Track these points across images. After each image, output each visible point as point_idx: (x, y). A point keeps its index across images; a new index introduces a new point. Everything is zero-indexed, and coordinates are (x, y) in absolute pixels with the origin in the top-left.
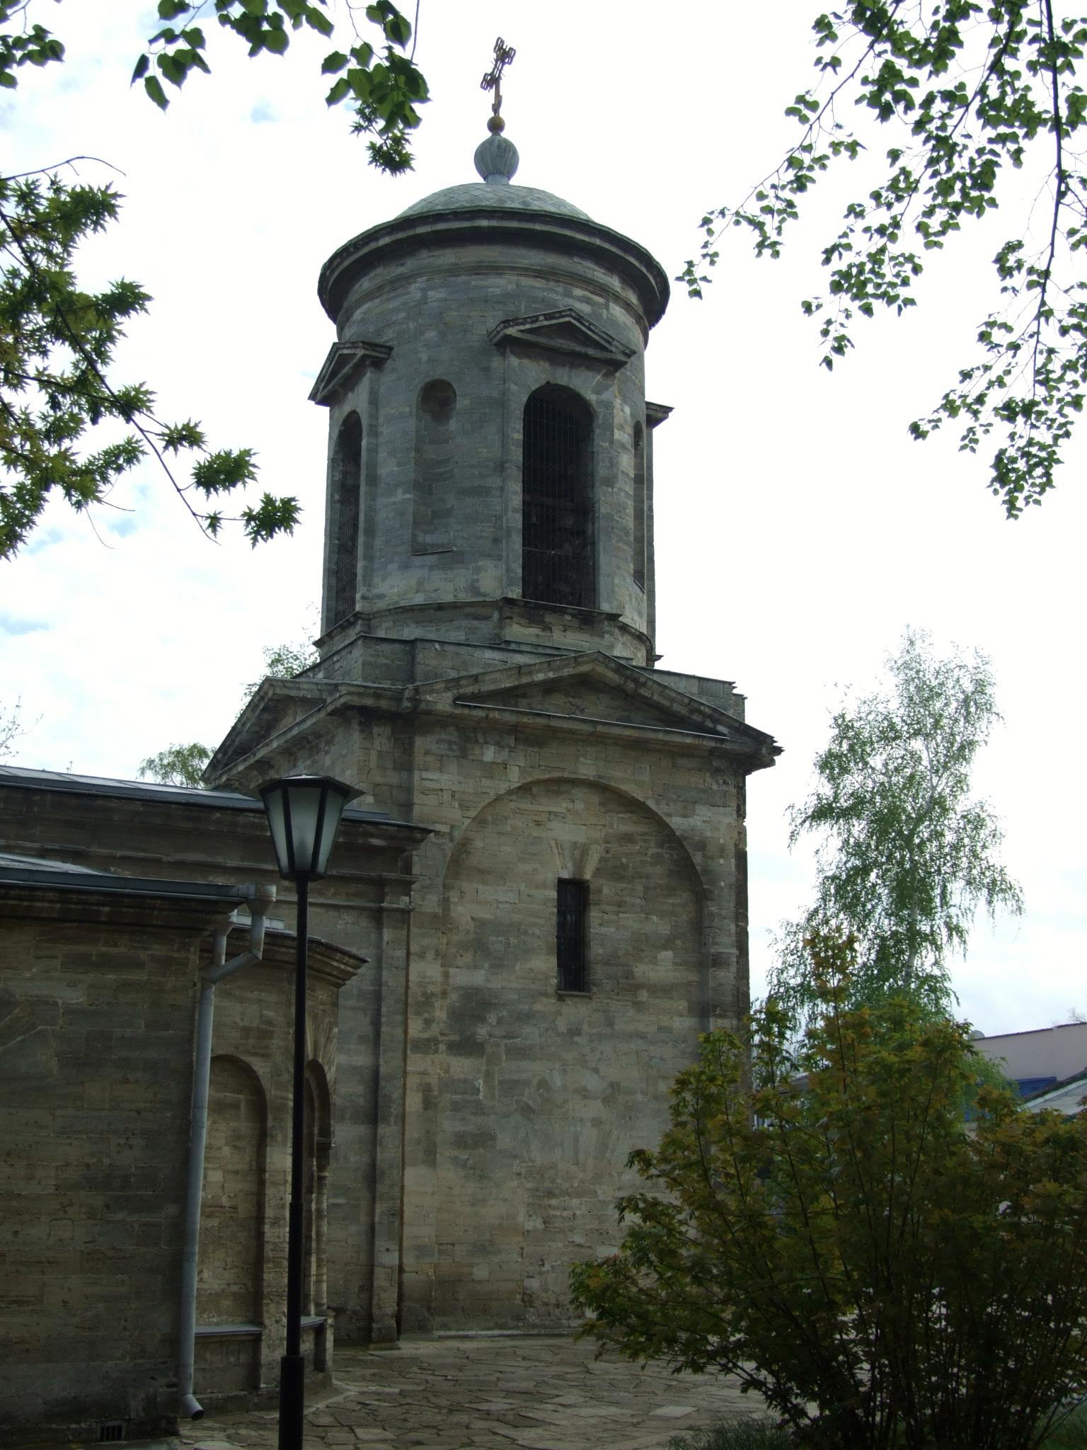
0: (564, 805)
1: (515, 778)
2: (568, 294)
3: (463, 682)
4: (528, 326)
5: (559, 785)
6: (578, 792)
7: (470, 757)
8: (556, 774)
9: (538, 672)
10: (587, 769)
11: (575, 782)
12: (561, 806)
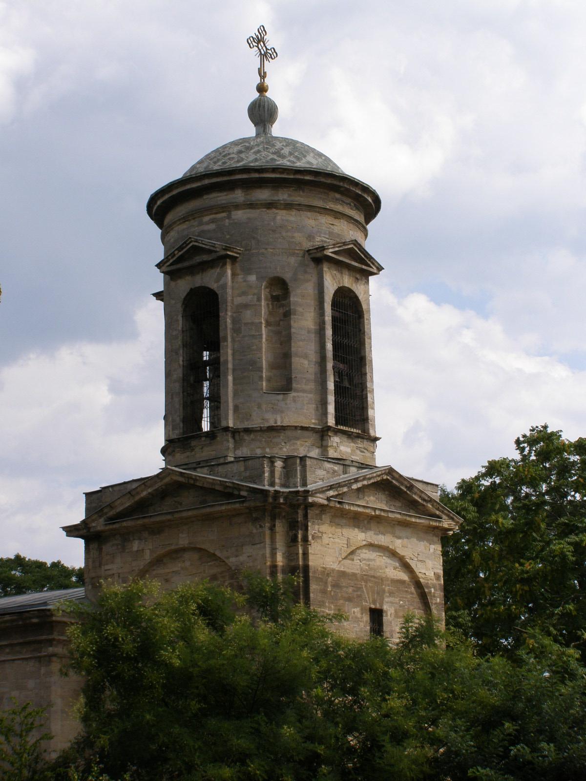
0: (180, 565)
1: (148, 557)
2: (201, 224)
3: (105, 510)
4: (171, 261)
5: (176, 554)
6: (187, 555)
7: (127, 551)
8: (168, 548)
9: (142, 491)
10: (183, 540)
11: (184, 550)
12: (177, 566)
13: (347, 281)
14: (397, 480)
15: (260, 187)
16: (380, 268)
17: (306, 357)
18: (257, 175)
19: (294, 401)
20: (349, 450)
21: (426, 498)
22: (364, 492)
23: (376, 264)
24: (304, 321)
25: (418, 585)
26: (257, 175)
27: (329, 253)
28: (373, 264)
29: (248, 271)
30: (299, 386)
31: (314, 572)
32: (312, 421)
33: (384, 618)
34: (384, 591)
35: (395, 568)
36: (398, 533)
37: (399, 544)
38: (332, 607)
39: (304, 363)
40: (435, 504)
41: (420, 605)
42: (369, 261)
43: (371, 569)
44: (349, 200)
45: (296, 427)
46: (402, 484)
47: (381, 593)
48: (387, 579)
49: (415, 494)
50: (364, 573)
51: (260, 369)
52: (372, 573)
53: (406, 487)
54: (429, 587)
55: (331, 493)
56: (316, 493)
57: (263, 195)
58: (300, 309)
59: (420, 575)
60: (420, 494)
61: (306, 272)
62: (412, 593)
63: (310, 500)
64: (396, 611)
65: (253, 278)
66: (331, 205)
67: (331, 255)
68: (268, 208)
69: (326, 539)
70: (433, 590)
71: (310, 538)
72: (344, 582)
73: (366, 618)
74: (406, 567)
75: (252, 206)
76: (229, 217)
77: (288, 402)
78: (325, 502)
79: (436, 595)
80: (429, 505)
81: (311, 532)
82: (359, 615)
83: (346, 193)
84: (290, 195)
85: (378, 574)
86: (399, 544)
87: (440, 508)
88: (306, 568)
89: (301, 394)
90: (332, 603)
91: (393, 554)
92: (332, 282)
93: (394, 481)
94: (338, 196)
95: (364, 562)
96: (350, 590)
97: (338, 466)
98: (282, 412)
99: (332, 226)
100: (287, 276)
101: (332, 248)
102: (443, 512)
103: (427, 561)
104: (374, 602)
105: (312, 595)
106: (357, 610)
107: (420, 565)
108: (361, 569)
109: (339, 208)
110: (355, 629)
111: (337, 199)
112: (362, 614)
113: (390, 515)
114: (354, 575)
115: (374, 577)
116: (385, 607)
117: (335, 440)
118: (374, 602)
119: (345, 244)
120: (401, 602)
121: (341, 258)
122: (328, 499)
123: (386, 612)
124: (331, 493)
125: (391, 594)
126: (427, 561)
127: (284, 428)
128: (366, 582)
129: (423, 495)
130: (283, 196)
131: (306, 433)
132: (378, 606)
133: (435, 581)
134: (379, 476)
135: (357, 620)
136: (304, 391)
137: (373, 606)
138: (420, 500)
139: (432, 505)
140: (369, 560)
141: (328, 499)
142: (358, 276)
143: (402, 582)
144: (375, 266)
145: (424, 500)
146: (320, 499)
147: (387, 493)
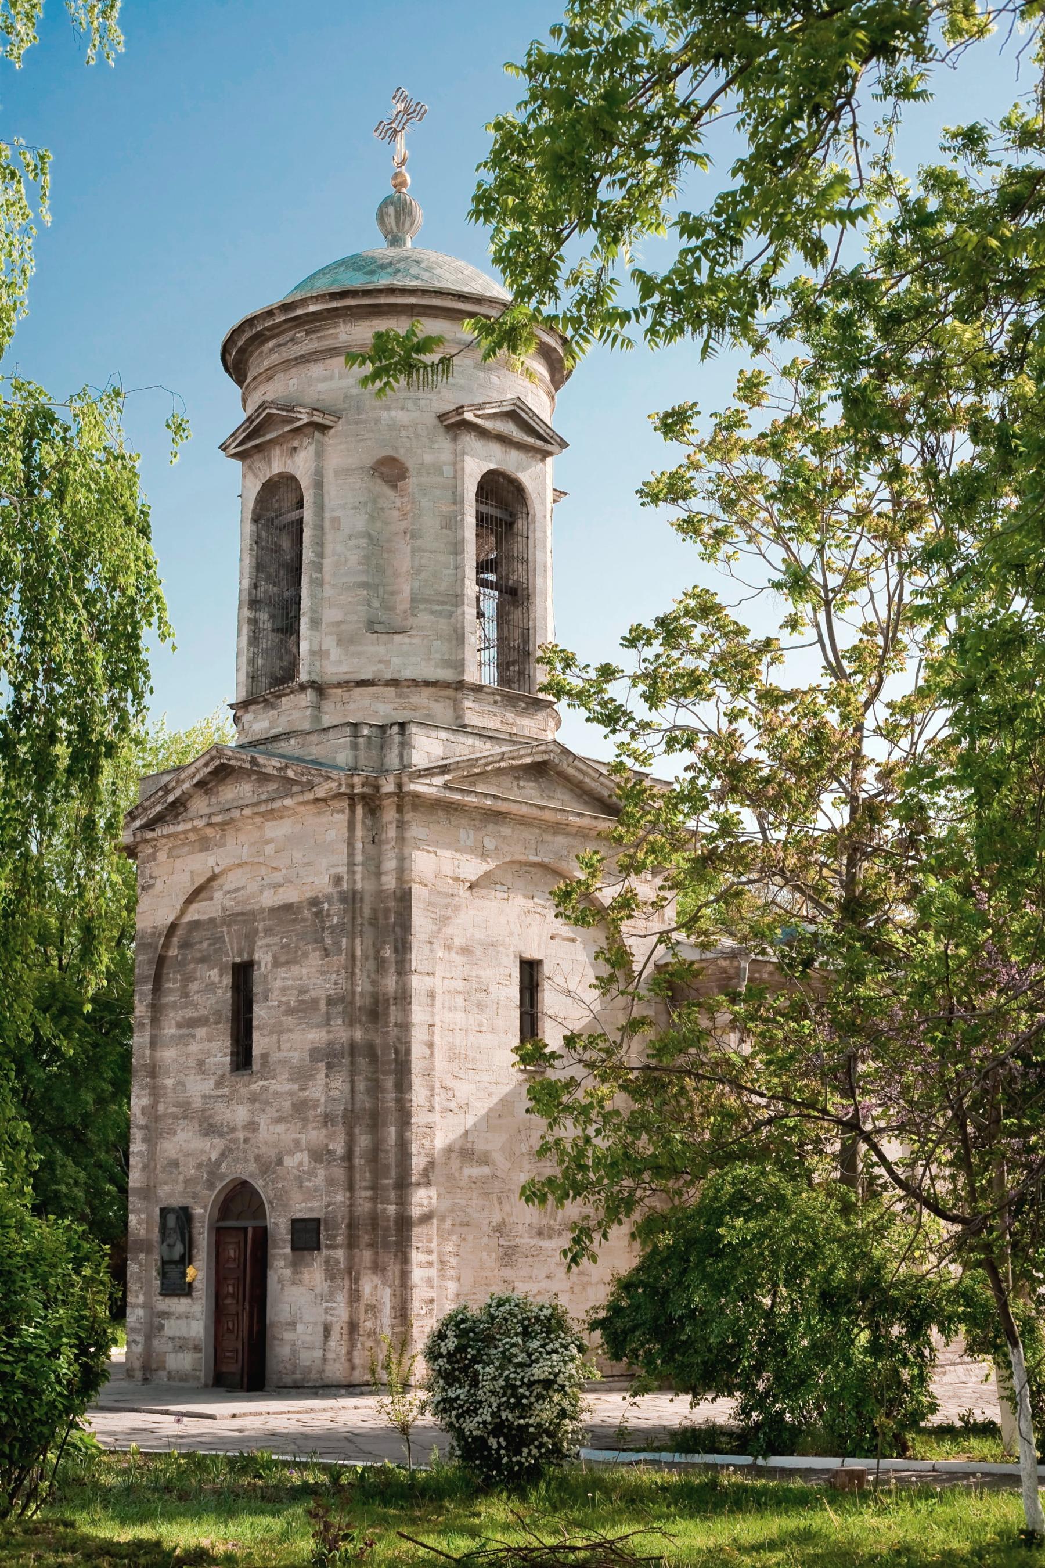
20: (266, 724)
47: (251, 937)
48: (262, 910)
52: (239, 909)
64: (274, 957)
70: (326, 906)
73: (227, 980)
82: (217, 979)
83: (274, 332)
94: (271, 344)
96: (205, 945)
106: (214, 974)
108: (224, 909)
109: (275, 358)
114: (212, 920)
116: (256, 956)
118: (240, 955)
124: (138, 823)
125: (268, 931)
128: (229, 926)
132: (246, 957)
134: (206, 765)
135: (211, 987)
137: (238, 960)
142: (296, 443)
143: (288, 908)
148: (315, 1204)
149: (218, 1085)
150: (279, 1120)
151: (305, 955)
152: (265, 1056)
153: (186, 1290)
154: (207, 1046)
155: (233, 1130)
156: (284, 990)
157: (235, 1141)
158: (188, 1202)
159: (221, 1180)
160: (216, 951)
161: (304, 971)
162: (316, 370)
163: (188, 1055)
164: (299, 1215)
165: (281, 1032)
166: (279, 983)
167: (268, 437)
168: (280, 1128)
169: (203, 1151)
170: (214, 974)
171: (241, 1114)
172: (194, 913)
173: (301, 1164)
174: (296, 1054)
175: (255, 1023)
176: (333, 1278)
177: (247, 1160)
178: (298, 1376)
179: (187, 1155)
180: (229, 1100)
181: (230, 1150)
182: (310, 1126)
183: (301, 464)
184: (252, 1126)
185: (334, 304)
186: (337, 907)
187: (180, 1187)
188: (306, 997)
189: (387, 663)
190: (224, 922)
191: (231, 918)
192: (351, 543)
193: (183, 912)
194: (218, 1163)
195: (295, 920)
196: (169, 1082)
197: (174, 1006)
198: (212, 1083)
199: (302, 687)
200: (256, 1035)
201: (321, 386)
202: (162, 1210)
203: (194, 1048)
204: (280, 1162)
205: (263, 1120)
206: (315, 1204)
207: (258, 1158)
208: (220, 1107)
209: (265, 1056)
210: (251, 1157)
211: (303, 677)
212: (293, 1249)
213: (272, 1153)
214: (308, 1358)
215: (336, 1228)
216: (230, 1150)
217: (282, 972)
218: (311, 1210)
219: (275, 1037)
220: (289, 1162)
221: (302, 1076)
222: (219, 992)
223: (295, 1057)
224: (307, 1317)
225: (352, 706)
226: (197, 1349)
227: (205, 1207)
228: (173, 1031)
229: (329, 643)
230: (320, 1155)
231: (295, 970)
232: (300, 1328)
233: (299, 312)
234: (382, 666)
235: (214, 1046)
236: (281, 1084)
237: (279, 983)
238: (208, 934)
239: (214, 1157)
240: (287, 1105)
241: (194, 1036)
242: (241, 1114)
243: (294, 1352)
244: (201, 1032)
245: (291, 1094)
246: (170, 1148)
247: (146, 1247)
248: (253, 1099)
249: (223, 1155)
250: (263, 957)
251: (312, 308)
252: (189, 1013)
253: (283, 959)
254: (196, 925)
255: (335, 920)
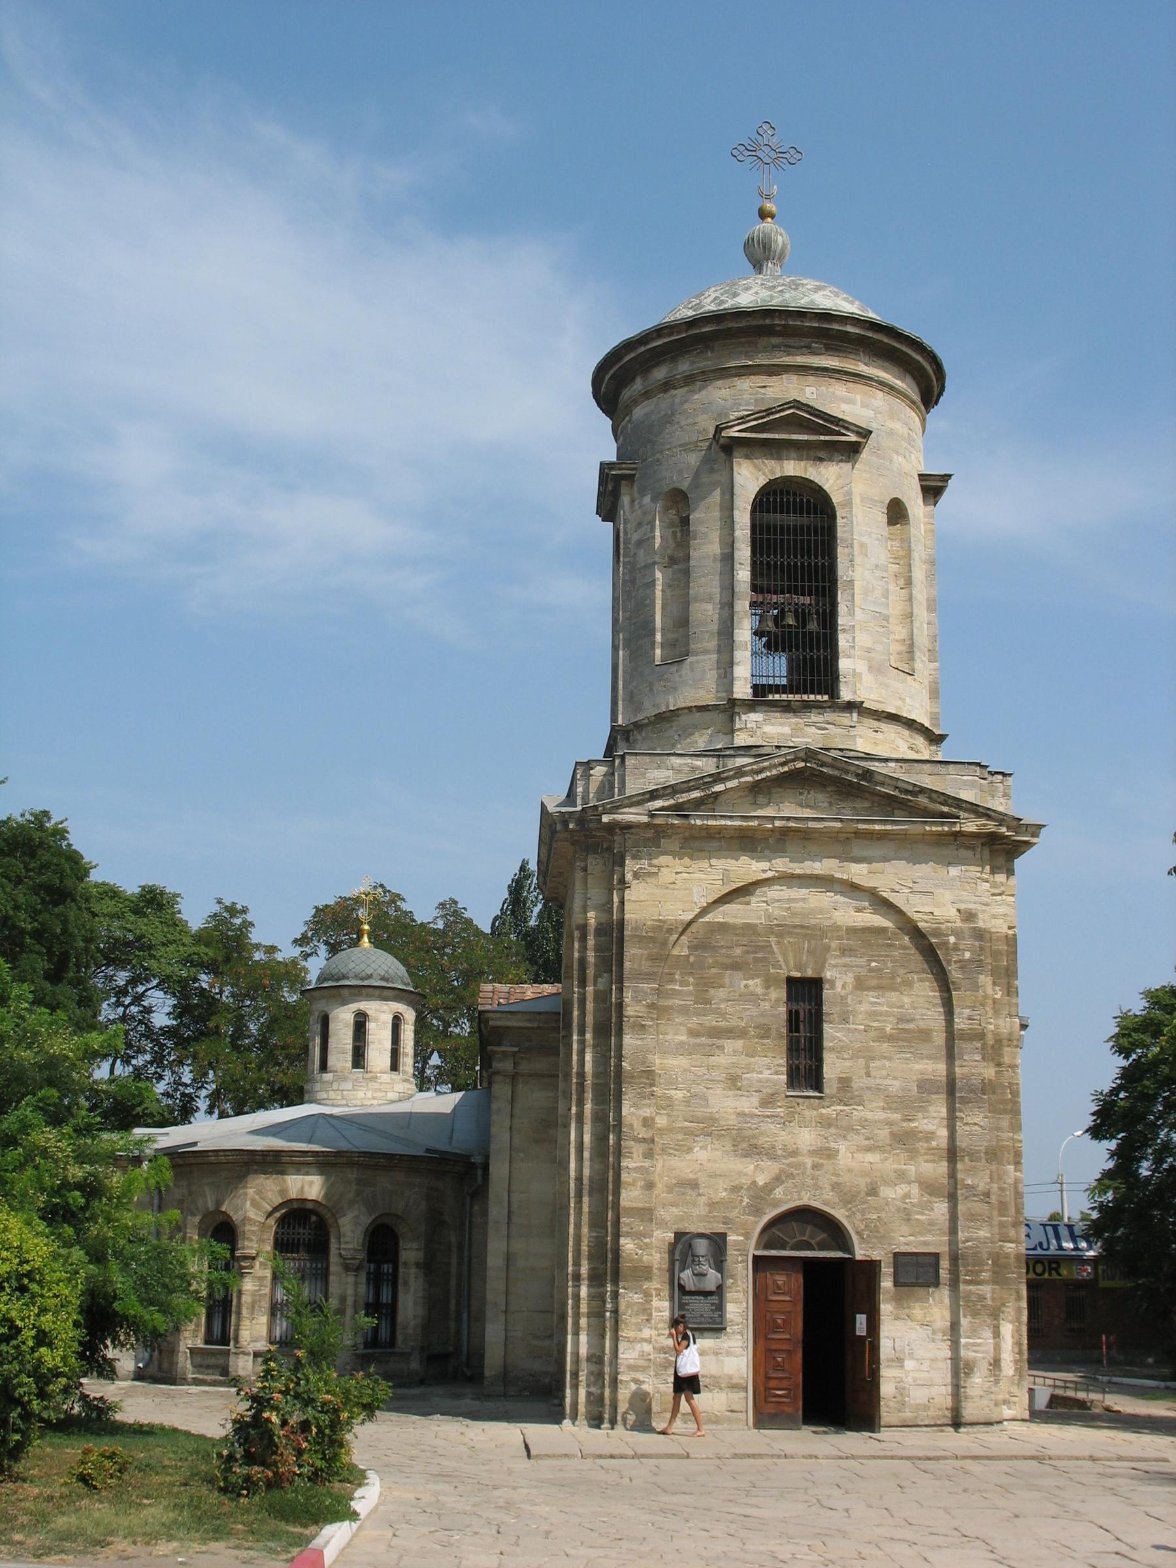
13: (792, 468)
14: (832, 766)
15: (657, 364)
16: (866, 434)
17: (709, 599)
18: (642, 349)
19: (692, 669)
20: (786, 730)
21: (910, 788)
22: (770, 793)
23: (851, 427)
24: (706, 547)
25: (917, 934)
26: (642, 349)
27: (733, 433)
28: (847, 429)
29: (642, 493)
30: (698, 645)
31: (636, 929)
32: (707, 694)
33: (827, 993)
34: (828, 949)
35: (858, 910)
36: (857, 851)
37: (858, 872)
38: (691, 980)
39: (706, 613)
40: (934, 796)
41: (926, 966)
42: (837, 425)
43: (794, 914)
44: (805, 341)
45: (689, 708)
46: (847, 772)
48: (836, 928)
49: (882, 784)
50: (775, 922)
51: (652, 633)
53: (857, 775)
54: (937, 933)
55: (658, 804)
56: (618, 807)
57: (660, 374)
58: (703, 529)
59: (916, 917)
60: (894, 783)
61: (712, 470)
62: (905, 948)
63: (605, 819)
65: (647, 499)
66: (762, 360)
67: (737, 435)
68: (666, 391)
69: (666, 875)
70: (952, 939)
71: (629, 877)
72: (720, 940)
73: (781, 993)
74: (884, 905)
75: (647, 395)
76: (630, 421)
77: (683, 672)
78: (645, 819)
79: (961, 947)
80: (923, 800)
81: (631, 865)
83: (787, 332)
84: (693, 363)
85: (813, 922)
86: (858, 872)
87: (950, 801)
88: (621, 923)
89: (701, 657)
90: (691, 974)
91: (852, 888)
92: (750, 478)
93: (825, 770)
94: (775, 340)
95: (776, 904)
96: (738, 951)
97: (705, 759)
98: (675, 689)
99: (762, 390)
100: (684, 485)
101: (738, 424)
102: (959, 807)
103: (938, 891)
104: (798, 968)
105: (627, 965)
106: (756, 985)
107: (915, 899)
108: (769, 916)
110: (748, 1013)
111: (774, 347)
112: (768, 988)
113: (811, 825)
114: (748, 926)
115: (802, 927)
116: (828, 975)
117: (753, 718)
118: (798, 968)
119: (769, 411)
120: (873, 964)
121: (764, 436)
122: (651, 815)
123: (832, 983)
125: (844, 951)
126: (937, 891)
127: (676, 713)
128: (780, 935)
129: (900, 784)
130: (684, 366)
131: (707, 716)
132: (810, 973)
133: (959, 924)
135: (753, 998)
136: (706, 652)
137: (796, 974)
138: (896, 793)
139: (930, 798)
140: (790, 900)
141: (651, 815)
142: (822, 454)
143: (882, 931)
144: (853, 431)
145: (907, 792)
146: (631, 815)
147: (829, 789)
148: (929, 1238)
149: (767, 1102)
150: (869, 1149)
151: (909, 984)
152: (845, 1083)
153: (716, 1327)
154: (744, 1060)
155: (794, 1153)
156: (873, 1015)
157: (798, 1166)
158: (720, 1228)
159: (775, 1205)
160: (756, 960)
161: (906, 1000)
162: (839, 389)
163: (710, 1068)
164: (903, 1249)
165: (873, 1059)
166: (863, 1008)
167: (795, 437)
168: (871, 1157)
169: (740, 1174)
170: (756, 985)
171: (807, 1138)
172: (717, 916)
173: (908, 1195)
174: (896, 1083)
175: (827, 1043)
176: (975, 1314)
177: (817, 1187)
178: (908, 1414)
179: (714, 1175)
180: (786, 1122)
181: (791, 1176)
182: (921, 1159)
183: (828, 476)
184: (830, 1154)
185: (870, 334)
186: (968, 942)
187: (701, 1210)
188: (911, 1026)
189: (903, 700)
190: (770, 930)
191: (781, 930)
192: (878, 573)
193: (704, 911)
194: (769, 1188)
195: (889, 945)
196: (678, 1095)
197: (684, 1011)
198: (755, 1100)
199: (851, 706)
200: (829, 1059)
201: (844, 407)
202: (679, 1235)
203: (722, 1060)
204: (873, 1191)
205: (842, 1147)
206: (929, 1238)
207: (836, 1186)
208: (770, 1127)
209: (845, 1083)
210: (825, 1182)
211: (846, 695)
212: (896, 1284)
213: (862, 1183)
214: (918, 1396)
215: (980, 1263)
216: (791, 1176)
217: (871, 997)
218: (925, 1243)
219: (862, 1061)
220: (887, 1192)
221: (906, 1104)
222: (766, 1005)
223: (895, 1086)
224: (919, 1353)
225: (880, 736)
226: (733, 1387)
227: (747, 1235)
228: (684, 1038)
229: (861, 666)
230: (929, 1188)
231: (893, 996)
232: (909, 1364)
233: (836, 326)
234: (900, 703)
235: (759, 1061)
236: (873, 1112)
237: (863, 1008)
238: (745, 940)
239: (761, 1183)
240: (883, 1134)
241: (721, 1048)
242: (807, 1138)
243: (901, 1390)
244: (730, 1045)
245: (889, 1123)
246: (683, 1166)
247: (645, 1273)
248: (826, 1123)
249: (778, 1180)
250: (839, 980)
251: (850, 329)
252: (711, 1021)
253: (874, 982)
254: (723, 927)
255: (967, 955)
